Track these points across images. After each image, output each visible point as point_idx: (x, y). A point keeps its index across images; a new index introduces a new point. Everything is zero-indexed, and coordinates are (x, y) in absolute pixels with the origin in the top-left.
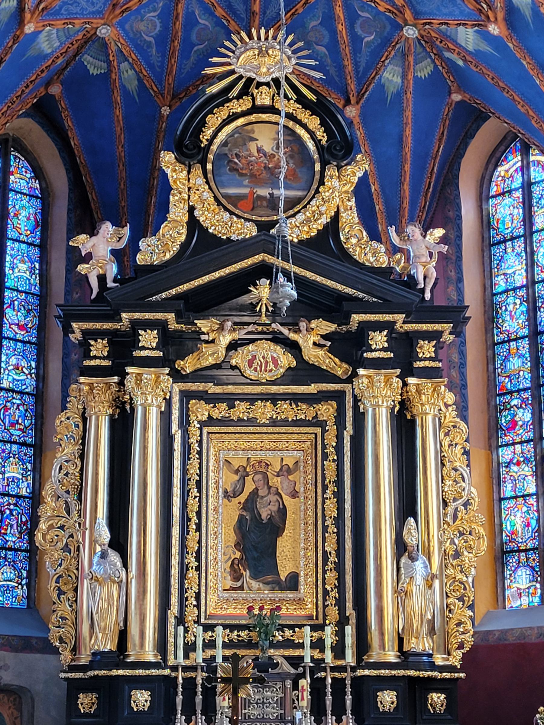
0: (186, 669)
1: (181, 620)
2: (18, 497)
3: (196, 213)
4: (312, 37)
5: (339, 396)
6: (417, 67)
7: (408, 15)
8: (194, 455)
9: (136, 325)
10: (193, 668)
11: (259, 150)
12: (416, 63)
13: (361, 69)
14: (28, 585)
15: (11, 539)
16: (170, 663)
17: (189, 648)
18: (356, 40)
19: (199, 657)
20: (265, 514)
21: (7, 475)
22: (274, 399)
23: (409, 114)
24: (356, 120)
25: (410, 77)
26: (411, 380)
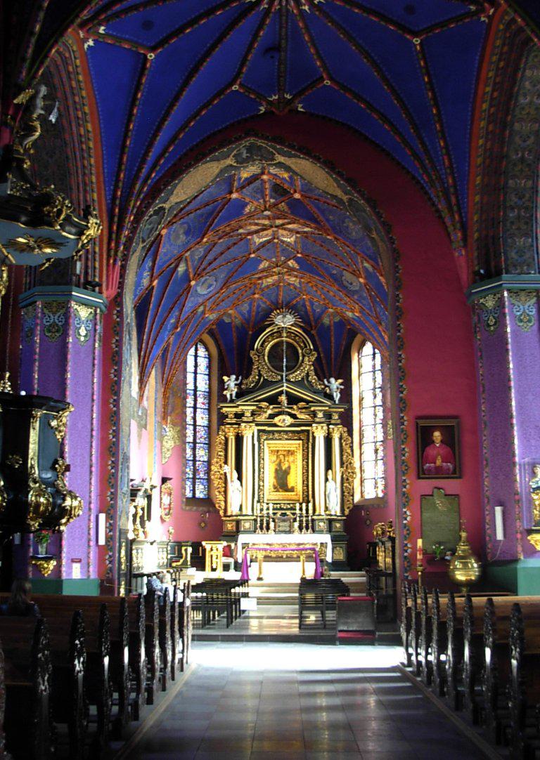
0: (260, 517)
1: (258, 502)
2: (204, 461)
5: (308, 431)
7: (330, 305)
10: (263, 516)
14: (208, 490)
15: (202, 475)
16: (255, 514)
17: (262, 510)
19: (265, 512)
20: (284, 468)
26: (331, 426)
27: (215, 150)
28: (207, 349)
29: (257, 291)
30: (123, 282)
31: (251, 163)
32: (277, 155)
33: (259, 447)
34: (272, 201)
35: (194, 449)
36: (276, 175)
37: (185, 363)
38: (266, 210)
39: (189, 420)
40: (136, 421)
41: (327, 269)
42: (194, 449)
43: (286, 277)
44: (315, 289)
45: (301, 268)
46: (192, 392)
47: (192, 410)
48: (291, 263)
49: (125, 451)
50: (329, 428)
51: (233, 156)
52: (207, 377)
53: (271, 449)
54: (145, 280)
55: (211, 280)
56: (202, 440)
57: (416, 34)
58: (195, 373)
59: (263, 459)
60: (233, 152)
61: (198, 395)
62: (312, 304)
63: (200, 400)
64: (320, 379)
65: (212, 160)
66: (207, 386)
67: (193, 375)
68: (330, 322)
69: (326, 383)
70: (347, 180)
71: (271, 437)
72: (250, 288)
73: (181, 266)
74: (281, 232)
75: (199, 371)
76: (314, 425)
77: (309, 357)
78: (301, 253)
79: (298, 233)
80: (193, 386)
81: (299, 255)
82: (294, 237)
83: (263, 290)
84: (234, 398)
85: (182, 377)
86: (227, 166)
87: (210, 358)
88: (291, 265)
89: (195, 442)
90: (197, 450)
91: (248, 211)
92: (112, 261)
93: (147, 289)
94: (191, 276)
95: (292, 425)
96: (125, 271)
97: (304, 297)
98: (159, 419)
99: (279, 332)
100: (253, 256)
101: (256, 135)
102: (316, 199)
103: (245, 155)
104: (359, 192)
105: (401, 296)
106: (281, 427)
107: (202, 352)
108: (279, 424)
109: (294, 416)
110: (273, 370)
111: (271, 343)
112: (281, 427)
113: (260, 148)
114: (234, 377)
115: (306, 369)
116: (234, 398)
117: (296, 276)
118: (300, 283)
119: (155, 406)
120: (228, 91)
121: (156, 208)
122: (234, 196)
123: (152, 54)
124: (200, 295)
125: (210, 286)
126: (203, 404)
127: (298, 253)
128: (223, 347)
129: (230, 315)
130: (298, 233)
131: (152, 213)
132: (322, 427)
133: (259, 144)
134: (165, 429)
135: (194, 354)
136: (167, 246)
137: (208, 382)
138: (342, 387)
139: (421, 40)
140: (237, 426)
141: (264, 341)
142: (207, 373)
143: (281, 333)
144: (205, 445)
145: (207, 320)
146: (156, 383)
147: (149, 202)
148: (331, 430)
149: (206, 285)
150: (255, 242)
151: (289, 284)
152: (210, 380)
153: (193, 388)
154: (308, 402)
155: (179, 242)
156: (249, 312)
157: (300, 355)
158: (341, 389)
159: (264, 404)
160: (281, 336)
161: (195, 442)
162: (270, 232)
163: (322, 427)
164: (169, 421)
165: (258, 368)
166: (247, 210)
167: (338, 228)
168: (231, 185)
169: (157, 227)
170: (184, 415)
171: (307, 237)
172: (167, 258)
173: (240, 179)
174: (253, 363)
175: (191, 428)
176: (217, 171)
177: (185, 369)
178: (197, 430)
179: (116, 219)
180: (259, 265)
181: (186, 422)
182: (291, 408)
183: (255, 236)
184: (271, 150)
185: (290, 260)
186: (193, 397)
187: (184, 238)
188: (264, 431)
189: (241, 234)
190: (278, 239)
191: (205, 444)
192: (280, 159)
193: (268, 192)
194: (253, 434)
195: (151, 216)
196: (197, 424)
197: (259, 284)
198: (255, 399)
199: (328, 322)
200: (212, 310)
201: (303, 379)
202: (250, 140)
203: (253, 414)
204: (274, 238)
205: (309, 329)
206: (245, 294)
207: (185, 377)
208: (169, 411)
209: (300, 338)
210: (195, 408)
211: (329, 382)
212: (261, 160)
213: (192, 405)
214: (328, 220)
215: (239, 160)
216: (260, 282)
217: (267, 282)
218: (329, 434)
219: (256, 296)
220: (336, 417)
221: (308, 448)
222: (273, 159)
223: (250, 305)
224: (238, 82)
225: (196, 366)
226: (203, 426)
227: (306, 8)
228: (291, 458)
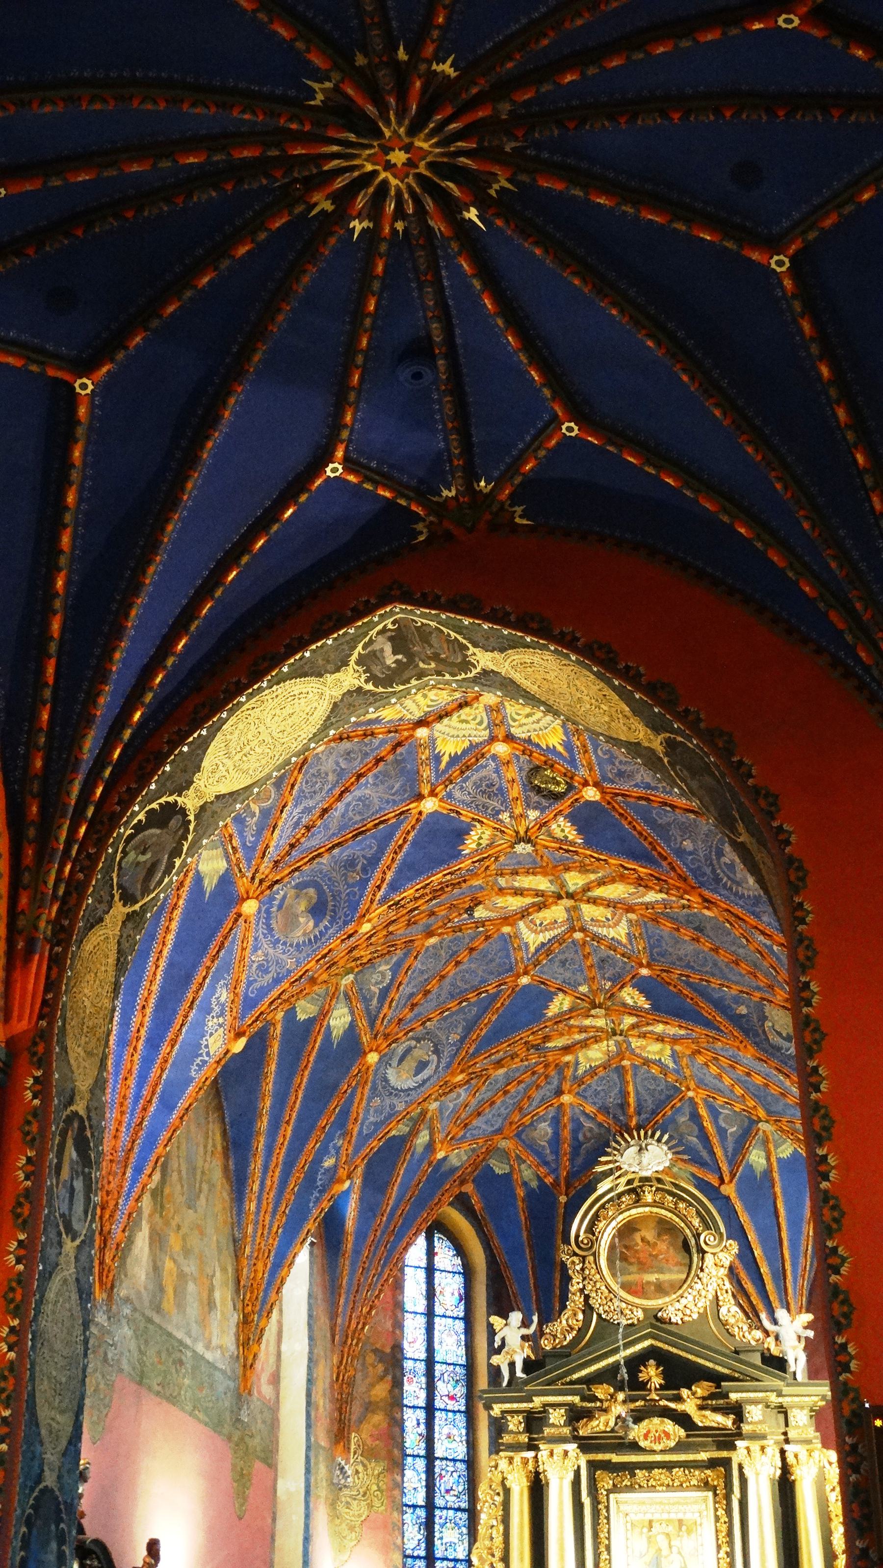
2: (456, 1560)
3: (591, 1302)
4: (683, 1129)
6: (779, 1150)
7: (762, 1113)
8: (603, 1520)
9: (545, 1405)
11: (643, 1240)
12: (776, 1147)
13: (729, 1154)
18: (722, 1132)
21: (444, 1541)
22: (669, 1466)
23: (778, 1190)
24: (733, 1196)
25: (773, 1159)
27: (303, 645)
28: (460, 1250)
29: (566, 1086)
30: (57, 997)
31: (414, 682)
32: (472, 650)
33: (596, 1513)
34: (533, 814)
35: (429, 1525)
36: (529, 741)
37: (398, 1286)
38: (520, 840)
39: (413, 1440)
40: (229, 1438)
41: (720, 1005)
42: (429, 1525)
43: (635, 1043)
44: (714, 1069)
45: (656, 1008)
46: (421, 1367)
47: (421, 1415)
48: (630, 996)
49: (50, 1480)
50: (783, 1452)
51: (358, 663)
52: (460, 1326)
53: (632, 1517)
54: (211, 1040)
55: (422, 1052)
56: (451, 1499)
57: (774, 245)
58: (430, 1314)
59: (608, 1548)
60: (355, 647)
61: (437, 1374)
62: (714, 1113)
63: (442, 1388)
64: (751, 1314)
65: (299, 673)
66: (462, 1351)
67: (422, 1320)
68: (768, 1159)
69: (767, 1324)
70: (651, 689)
71: (626, 1482)
72: (547, 1077)
73: (336, 1013)
74: (588, 911)
75: (438, 1310)
76: (739, 1443)
77: (714, 1254)
78: (649, 966)
79: (630, 909)
80: (424, 1349)
81: (644, 972)
82: (624, 924)
83: (579, 1081)
84: (519, 1374)
85: (389, 1325)
86: (349, 692)
87: (468, 1273)
88: (630, 1002)
89: (430, 1506)
90: (437, 1527)
91: (474, 846)
92: (20, 945)
93: (218, 1062)
94: (365, 1039)
95: (680, 1447)
96: (62, 971)
97: (691, 1094)
98: (323, 1439)
99: (635, 1191)
100: (525, 980)
101: (407, 598)
102: (640, 798)
103: (390, 659)
104: (682, 717)
105: (814, 987)
106: (653, 1452)
107: (446, 1257)
108: (642, 1444)
109: (683, 1420)
110: (623, 1294)
111: (614, 1224)
112: (653, 1452)
113: (424, 634)
114: (516, 1317)
115: (711, 1289)
116: (519, 1374)
117: (660, 1039)
118: (674, 1055)
119: (309, 1404)
120: (318, 482)
121: (155, 806)
122: (429, 805)
123: (85, 380)
124: (396, 1092)
125: (422, 1066)
126: (452, 1398)
127: (641, 965)
128: (496, 1242)
129: (505, 1155)
130: (630, 909)
131: (141, 816)
132: (763, 1449)
133: (420, 621)
134: (342, 1469)
135: (424, 1264)
136: (266, 946)
137: (463, 1337)
138: (811, 1334)
139: (792, 260)
140: (530, 1454)
141: (596, 1217)
142: (462, 1315)
143: (638, 1195)
144: (459, 1514)
145: (445, 1168)
146: (311, 1338)
147: (129, 789)
148: (790, 1459)
149: (410, 1064)
150: (527, 945)
151: (647, 1062)
152: (469, 1331)
153: (423, 1356)
154: (716, 1378)
155: (298, 935)
156: (556, 1141)
157: (694, 1250)
158: (807, 1338)
159: (601, 1391)
160: (638, 1202)
161: (430, 1506)
162: (558, 912)
163: (763, 1449)
164: (353, 1447)
165: (582, 1291)
166: (470, 844)
167: (708, 871)
168: (414, 778)
169: (171, 866)
170: (397, 1430)
171: (655, 920)
172: (268, 978)
173: (438, 758)
174: (570, 1279)
175: (421, 1464)
176: (323, 709)
177: (398, 1306)
178: (437, 1470)
179: (32, 832)
180: (547, 1007)
181: (402, 1448)
182: (678, 1399)
183: (521, 924)
184: (453, 634)
185: (622, 987)
186: (423, 1380)
187: (311, 924)
188: (607, 1466)
189: (483, 923)
190: (583, 930)
191: (459, 1509)
192: (483, 659)
193: (515, 791)
194: (577, 1473)
195: (139, 828)
196: (438, 1453)
197: (567, 1064)
198: (575, 1376)
199: (763, 1161)
200: (453, 1141)
201: (703, 1316)
202: (392, 614)
203: (575, 1416)
204: (572, 929)
205: (715, 1182)
206: (537, 1096)
207: (399, 1325)
208: (354, 1418)
209: (691, 1205)
210: (430, 1409)
211: (775, 1322)
212: (439, 673)
213: (422, 1402)
214: (680, 852)
215: (377, 670)
216: (568, 1058)
217: (589, 1060)
218: (786, 1469)
219: (566, 1099)
220: (801, 1419)
221: (729, 1511)
222: (466, 665)
223: (556, 1122)
224: (340, 454)
225: (431, 1295)
226: (454, 1460)
227: (472, 214)
228: (686, 1543)
